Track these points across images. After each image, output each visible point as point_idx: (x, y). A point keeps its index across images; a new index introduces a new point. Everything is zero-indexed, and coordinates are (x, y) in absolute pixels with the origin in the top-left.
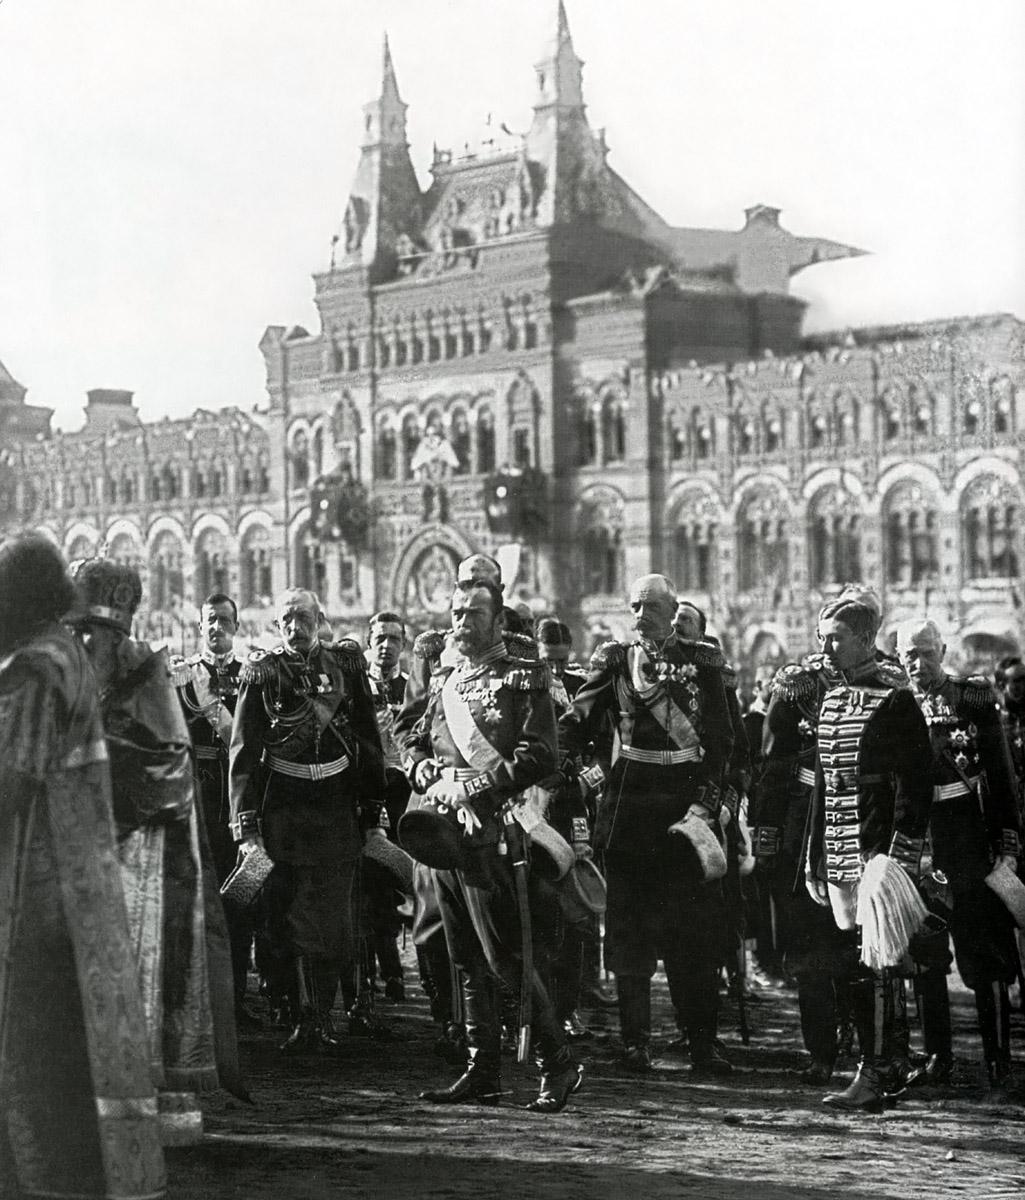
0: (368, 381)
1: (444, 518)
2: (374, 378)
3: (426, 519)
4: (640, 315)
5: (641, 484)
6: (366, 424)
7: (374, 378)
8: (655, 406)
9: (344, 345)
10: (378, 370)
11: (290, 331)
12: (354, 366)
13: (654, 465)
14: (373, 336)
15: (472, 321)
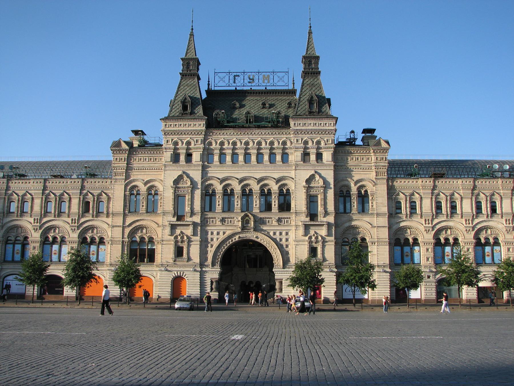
3: (244, 228)
5: (384, 221)
8: (391, 192)
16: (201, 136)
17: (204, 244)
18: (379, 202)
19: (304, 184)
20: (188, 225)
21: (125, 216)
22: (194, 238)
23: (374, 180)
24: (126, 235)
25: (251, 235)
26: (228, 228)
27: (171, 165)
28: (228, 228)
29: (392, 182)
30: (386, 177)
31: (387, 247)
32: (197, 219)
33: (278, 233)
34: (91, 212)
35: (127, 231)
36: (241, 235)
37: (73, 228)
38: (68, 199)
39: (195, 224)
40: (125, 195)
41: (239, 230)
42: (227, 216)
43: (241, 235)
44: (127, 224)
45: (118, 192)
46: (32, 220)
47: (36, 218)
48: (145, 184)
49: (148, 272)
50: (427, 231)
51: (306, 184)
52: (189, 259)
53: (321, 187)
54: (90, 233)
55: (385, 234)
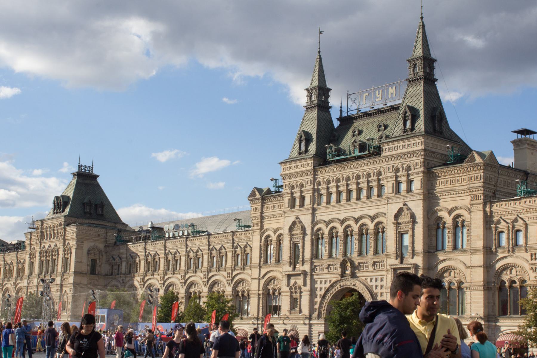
0: (310, 211)
1: (353, 275)
2: (314, 210)
3: (343, 275)
4: (481, 173)
5: (478, 259)
6: (309, 231)
7: (314, 210)
8: (488, 220)
9: (297, 195)
10: (315, 206)
11: (265, 190)
12: (302, 205)
13: (489, 251)
14: (314, 190)
15: (373, 180)
16: (310, 177)
17: (313, 293)
18: (475, 235)
19: (393, 220)
20: (299, 275)
21: (260, 267)
22: (303, 288)
23: (469, 206)
24: (261, 288)
25: (349, 283)
26: (332, 276)
27: (288, 211)
28: (332, 276)
29: (491, 207)
30: (481, 201)
31: (483, 292)
32: (307, 267)
33: (374, 280)
34: (192, 268)
35: (262, 281)
36: (342, 284)
37: (534, 267)
38: (524, 226)
39: (305, 273)
40: (261, 246)
41: (339, 278)
42: (332, 263)
43: (342, 284)
44: (262, 275)
45: (256, 243)
46: (225, 274)
47: (533, 253)
48: (450, 213)
49: (245, 326)
50: (205, 285)
51: (395, 220)
52: (300, 311)
53: (409, 222)
54: (507, 275)
55: (478, 276)
